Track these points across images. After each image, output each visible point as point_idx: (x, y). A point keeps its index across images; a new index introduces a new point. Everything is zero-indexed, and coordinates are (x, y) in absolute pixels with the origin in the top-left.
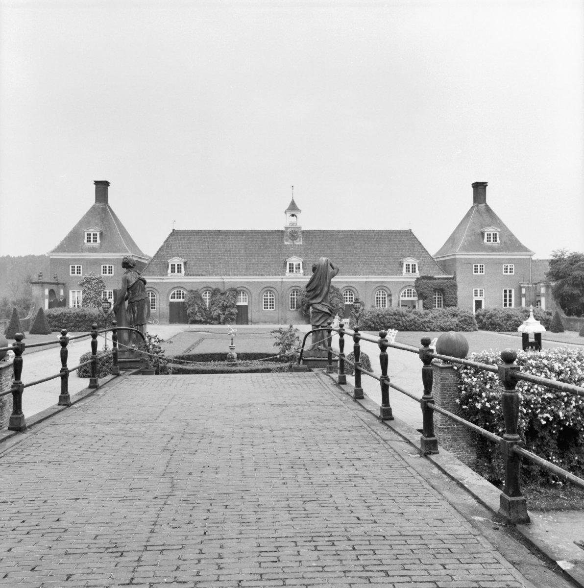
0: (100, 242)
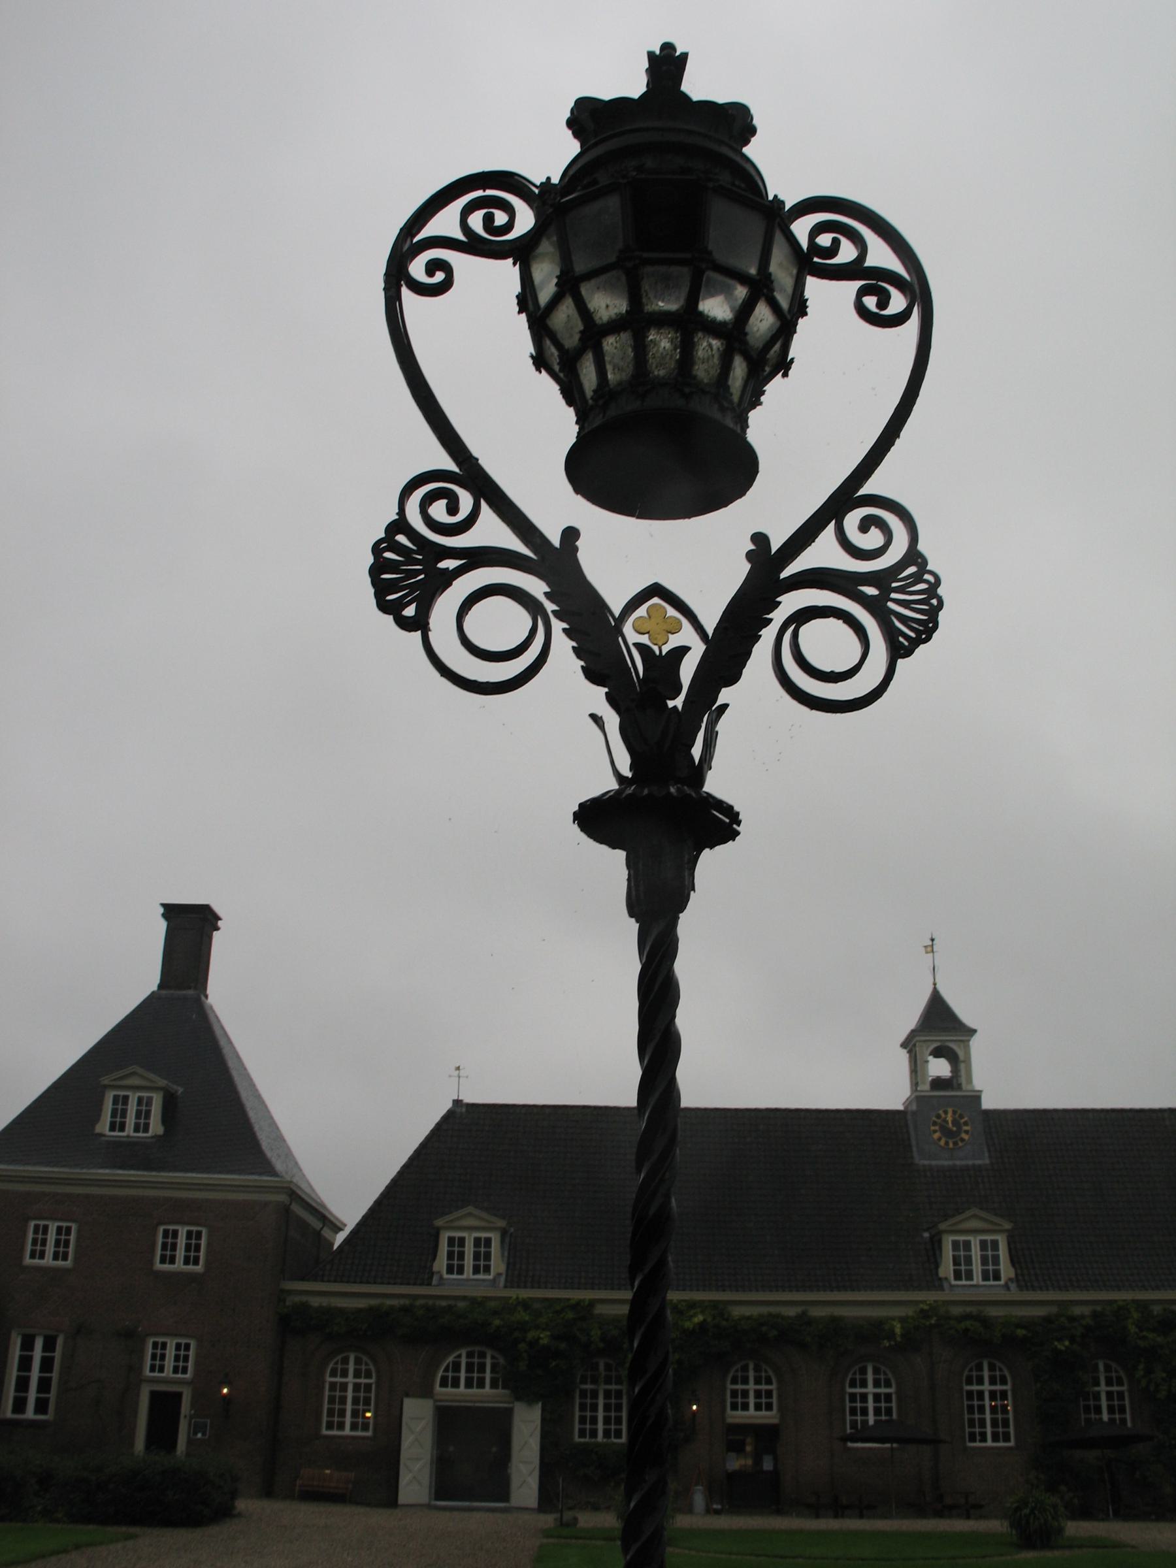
0: (160, 1130)
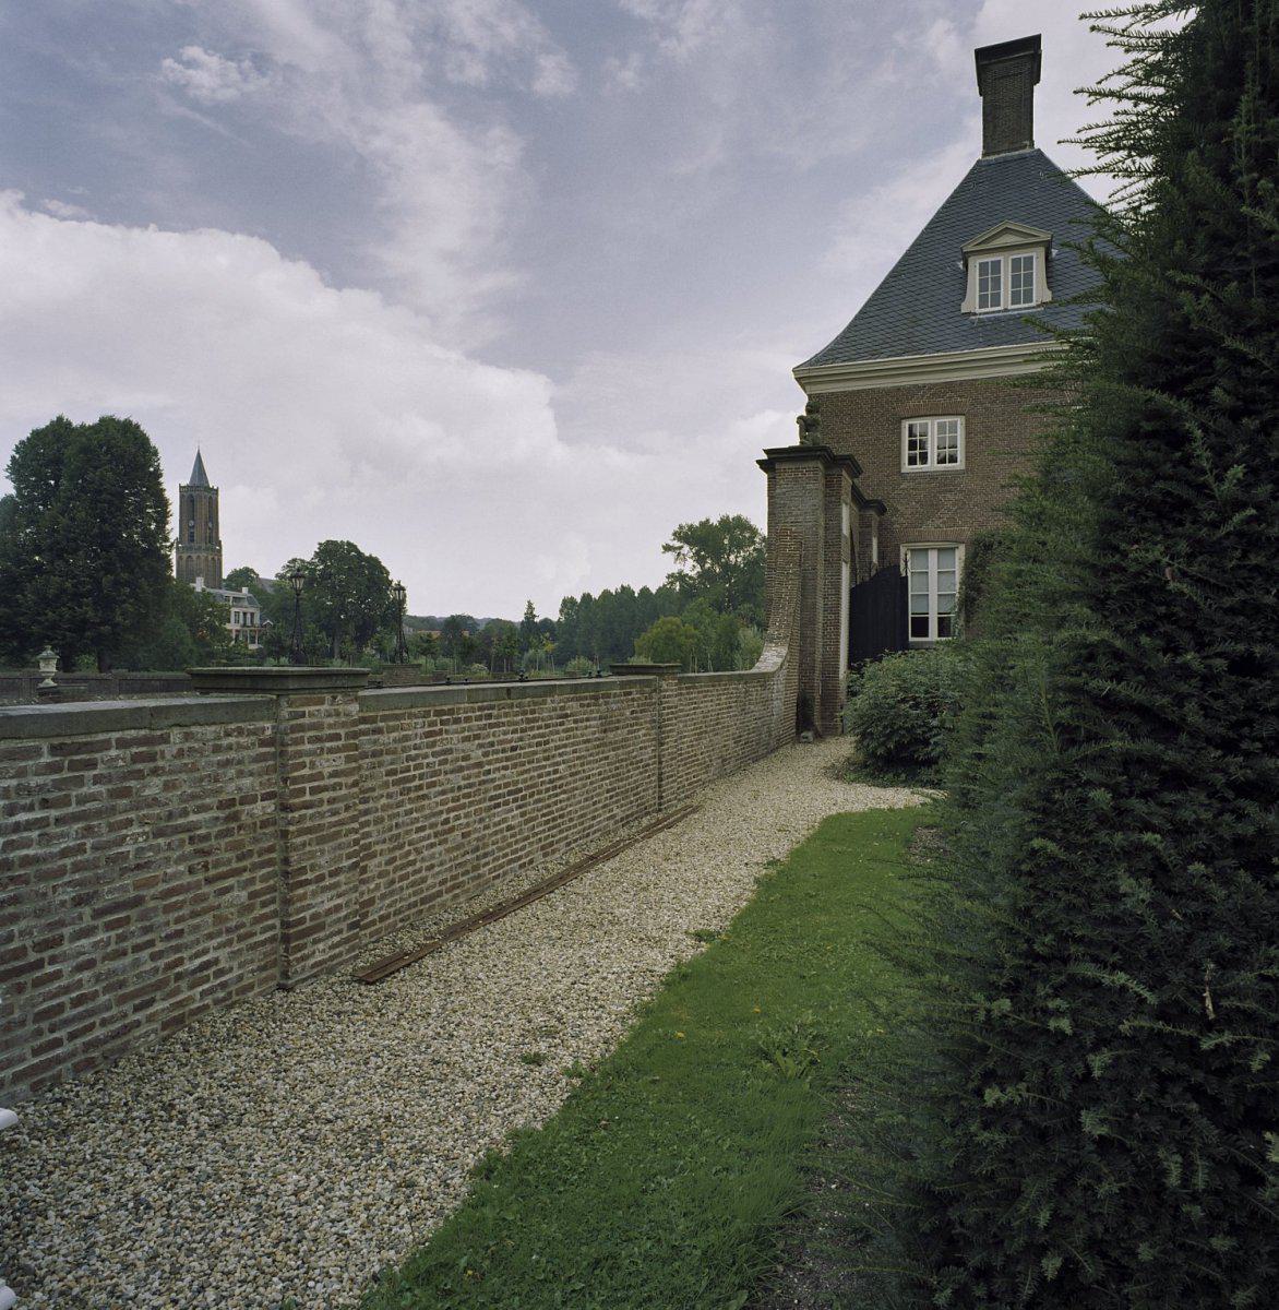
0: (1048, 296)
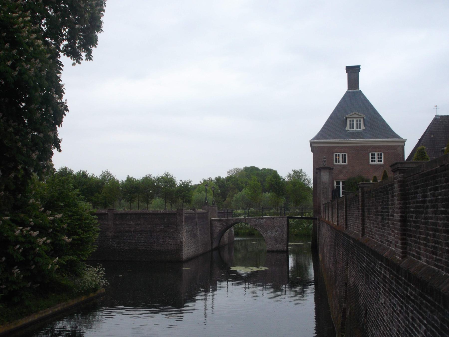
0: (364, 128)
